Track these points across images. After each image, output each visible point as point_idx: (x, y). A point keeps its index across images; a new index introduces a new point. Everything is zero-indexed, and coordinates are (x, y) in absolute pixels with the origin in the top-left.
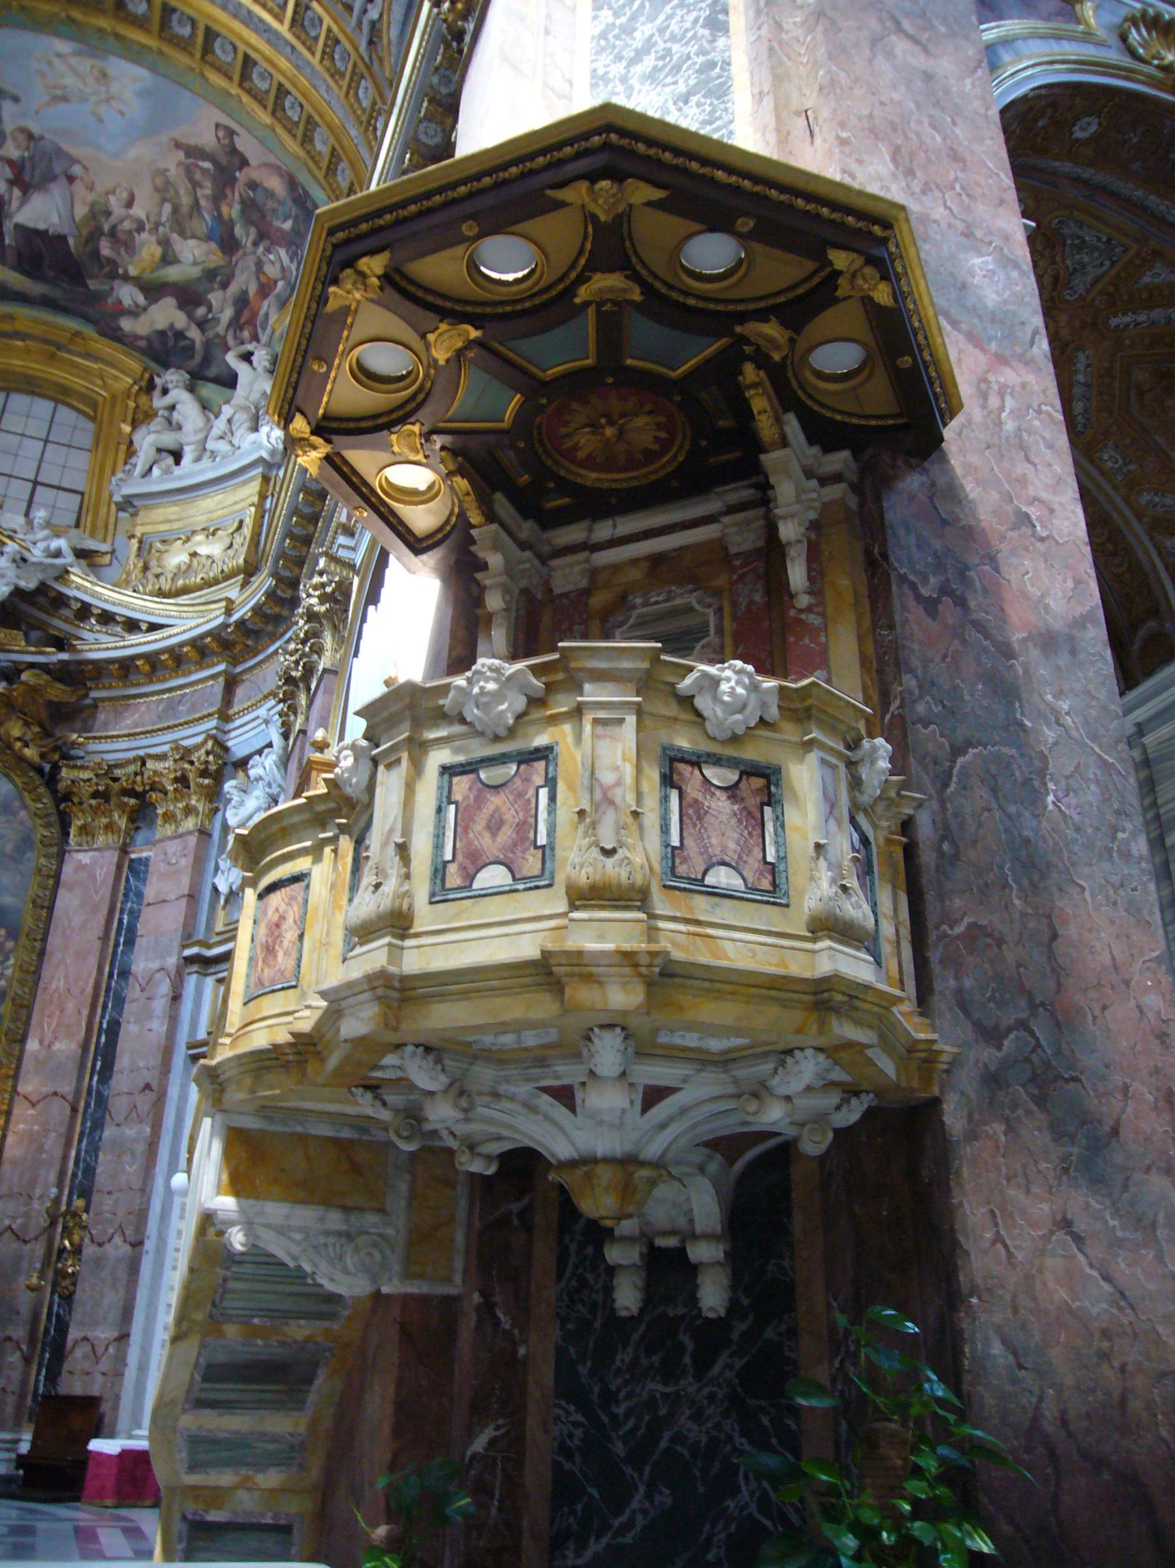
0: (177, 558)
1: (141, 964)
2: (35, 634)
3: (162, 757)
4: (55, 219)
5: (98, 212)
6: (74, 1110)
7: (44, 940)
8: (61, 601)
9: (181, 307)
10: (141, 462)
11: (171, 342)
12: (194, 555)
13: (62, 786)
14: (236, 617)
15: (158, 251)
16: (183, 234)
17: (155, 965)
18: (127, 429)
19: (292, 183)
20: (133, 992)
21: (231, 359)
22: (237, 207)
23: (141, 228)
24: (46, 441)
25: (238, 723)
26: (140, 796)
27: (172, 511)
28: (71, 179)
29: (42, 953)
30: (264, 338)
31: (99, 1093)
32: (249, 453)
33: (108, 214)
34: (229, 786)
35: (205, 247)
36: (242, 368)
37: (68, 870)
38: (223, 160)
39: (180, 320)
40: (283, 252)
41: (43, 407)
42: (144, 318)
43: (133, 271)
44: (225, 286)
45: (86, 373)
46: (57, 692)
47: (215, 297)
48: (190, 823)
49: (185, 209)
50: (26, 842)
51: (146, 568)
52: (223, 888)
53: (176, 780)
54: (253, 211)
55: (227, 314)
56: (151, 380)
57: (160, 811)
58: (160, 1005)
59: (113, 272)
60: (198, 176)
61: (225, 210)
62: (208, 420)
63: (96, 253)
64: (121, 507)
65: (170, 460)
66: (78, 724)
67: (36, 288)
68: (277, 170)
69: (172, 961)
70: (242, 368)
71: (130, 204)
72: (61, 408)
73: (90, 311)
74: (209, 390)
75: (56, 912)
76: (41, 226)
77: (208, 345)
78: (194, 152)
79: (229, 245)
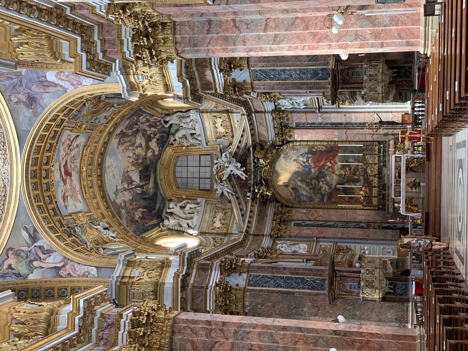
0: (221, 130)
1: (320, 121)
2: (248, 155)
3: (274, 124)
4: (136, 174)
5: (133, 164)
6: (349, 129)
7: (314, 141)
8: (235, 153)
9: (151, 141)
10: (194, 142)
11: (160, 141)
12: (221, 125)
13: (281, 143)
14: (245, 113)
15: (139, 148)
16: (135, 143)
17: (320, 118)
18: (184, 148)
19: (128, 118)
20: (325, 121)
21: (167, 126)
22: (130, 131)
23: (134, 154)
24: (187, 166)
25: (266, 109)
26: (282, 127)
27: (208, 133)
28: (128, 171)
29: (317, 141)
30: (160, 119)
31: (345, 125)
32: (197, 117)
33: (133, 161)
34: (283, 109)
35: (137, 137)
36: (170, 123)
37: (298, 139)
38: (121, 136)
39: (154, 140)
40: (140, 118)
41: (178, 169)
42: (154, 149)
43: (144, 154)
44: (146, 131)
45: (170, 160)
46: (258, 149)
47: (149, 133)
48: (290, 115)
49: (130, 144)
50: (293, 148)
51: (224, 136)
52: (304, 107)
53: (280, 120)
54: (130, 127)
55: (153, 129)
56: (170, 144)
57: (287, 122)
58: (328, 115)
59: (145, 158)
60: (123, 142)
61: (130, 134)
62: (181, 129)
63: (141, 163)
64: (207, 145)
65: (195, 136)
66: (264, 144)
67: (152, 176)
68: (125, 122)
69: (319, 114)
70: (170, 123)
71: (130, 157)
72: (178, 164)
73: (154, 162)
74: (173, 130)
75: (308, 139)
76: (139, 176)
77: (160, 133)
78: (119, 143)
79: (137, 131)
